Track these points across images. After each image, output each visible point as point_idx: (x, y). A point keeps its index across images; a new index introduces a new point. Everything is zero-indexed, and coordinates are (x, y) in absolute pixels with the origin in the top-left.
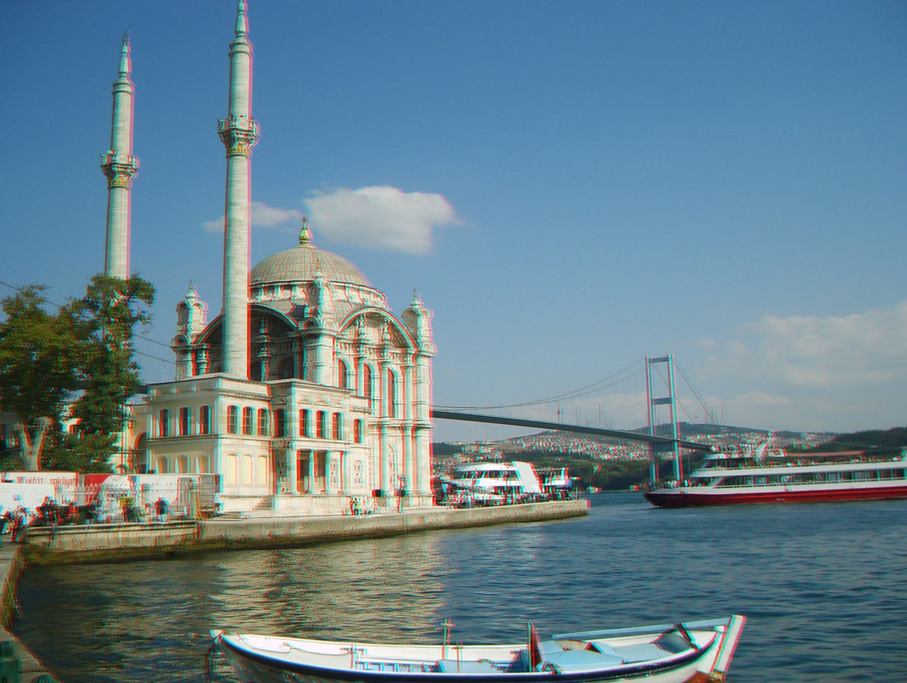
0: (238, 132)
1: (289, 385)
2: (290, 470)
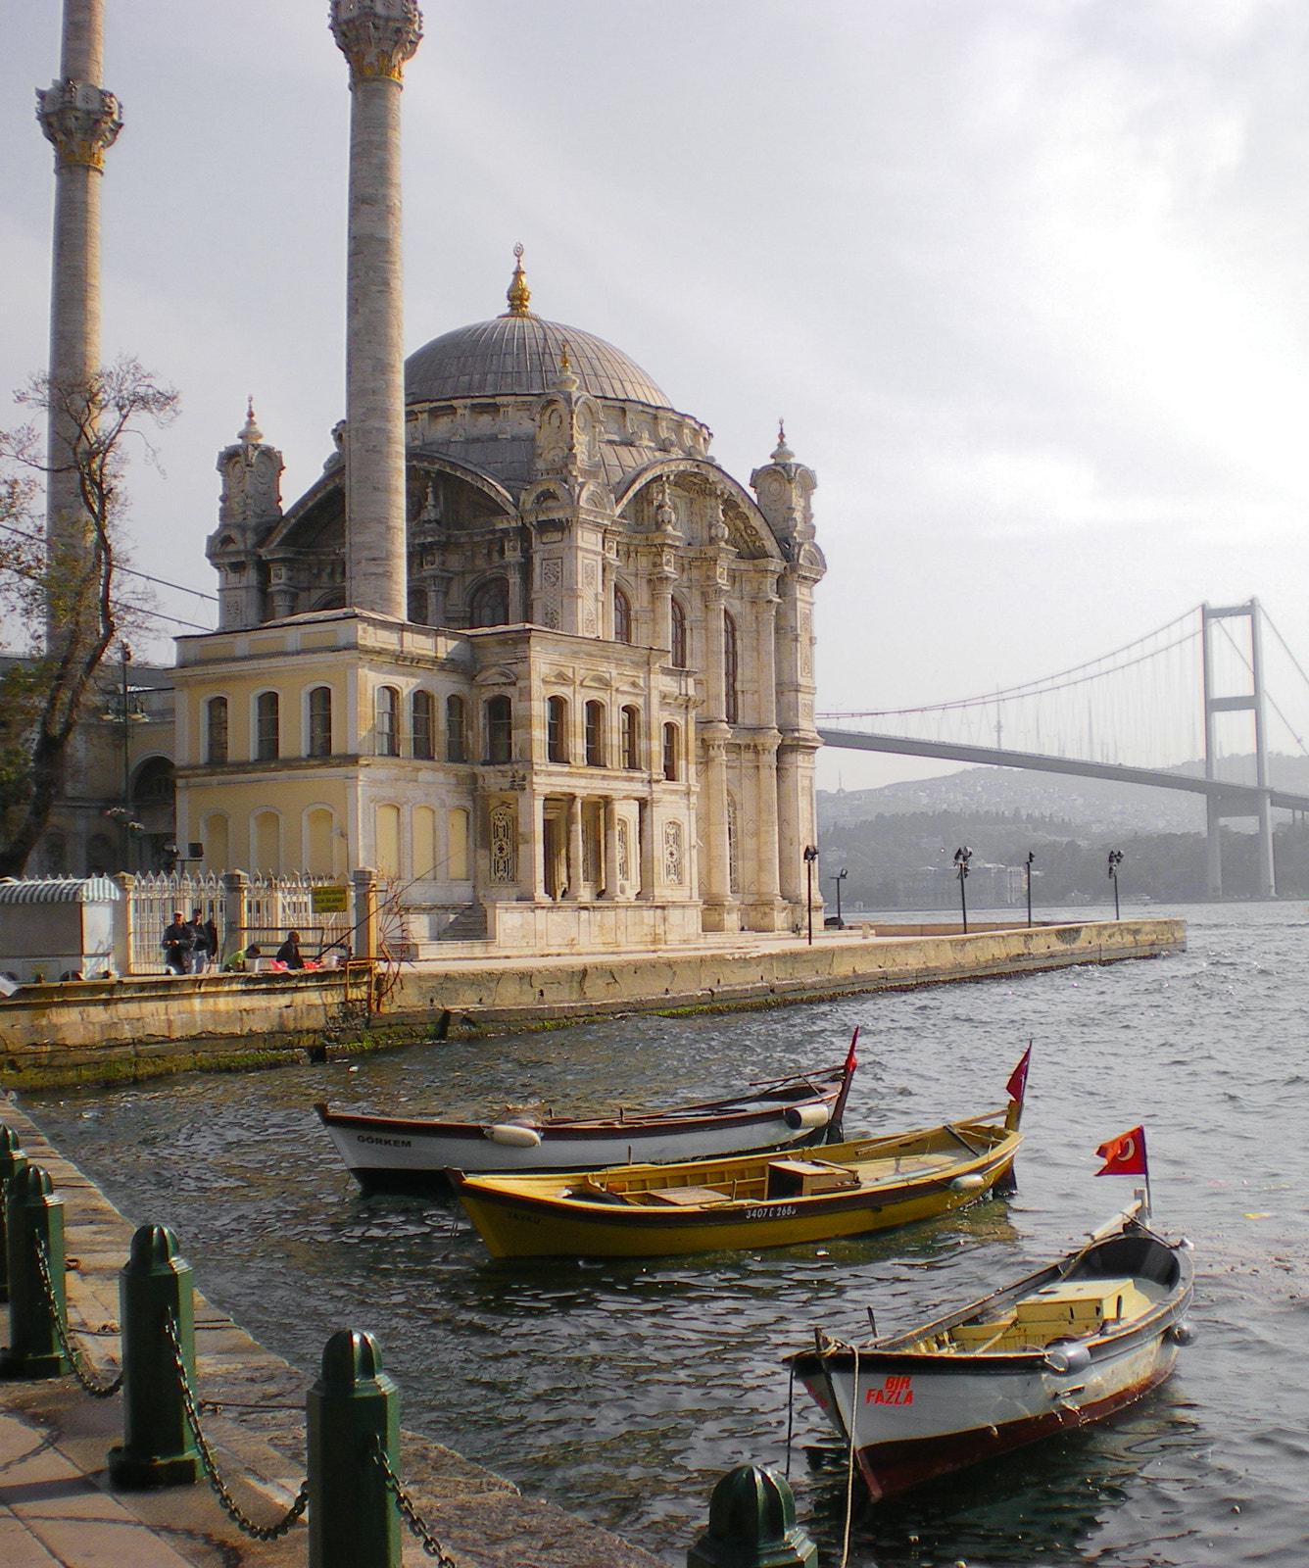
1: (524, 637)
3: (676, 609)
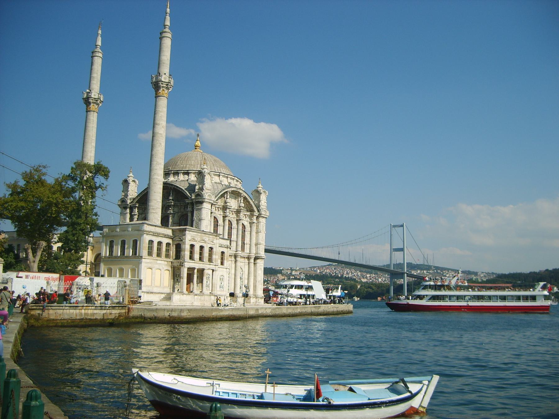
0: (162, 83)
1: (185, 230)
2: (183, 278)
3: (230, 223)
